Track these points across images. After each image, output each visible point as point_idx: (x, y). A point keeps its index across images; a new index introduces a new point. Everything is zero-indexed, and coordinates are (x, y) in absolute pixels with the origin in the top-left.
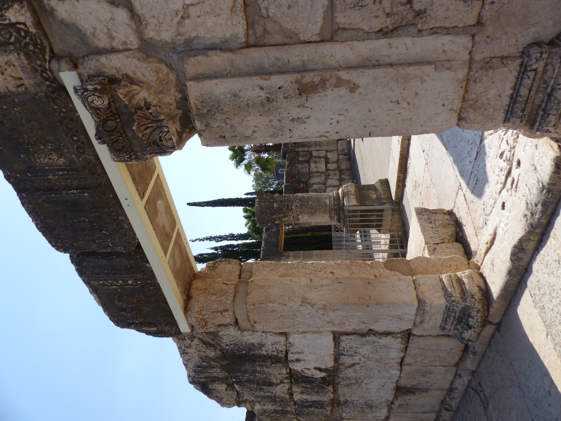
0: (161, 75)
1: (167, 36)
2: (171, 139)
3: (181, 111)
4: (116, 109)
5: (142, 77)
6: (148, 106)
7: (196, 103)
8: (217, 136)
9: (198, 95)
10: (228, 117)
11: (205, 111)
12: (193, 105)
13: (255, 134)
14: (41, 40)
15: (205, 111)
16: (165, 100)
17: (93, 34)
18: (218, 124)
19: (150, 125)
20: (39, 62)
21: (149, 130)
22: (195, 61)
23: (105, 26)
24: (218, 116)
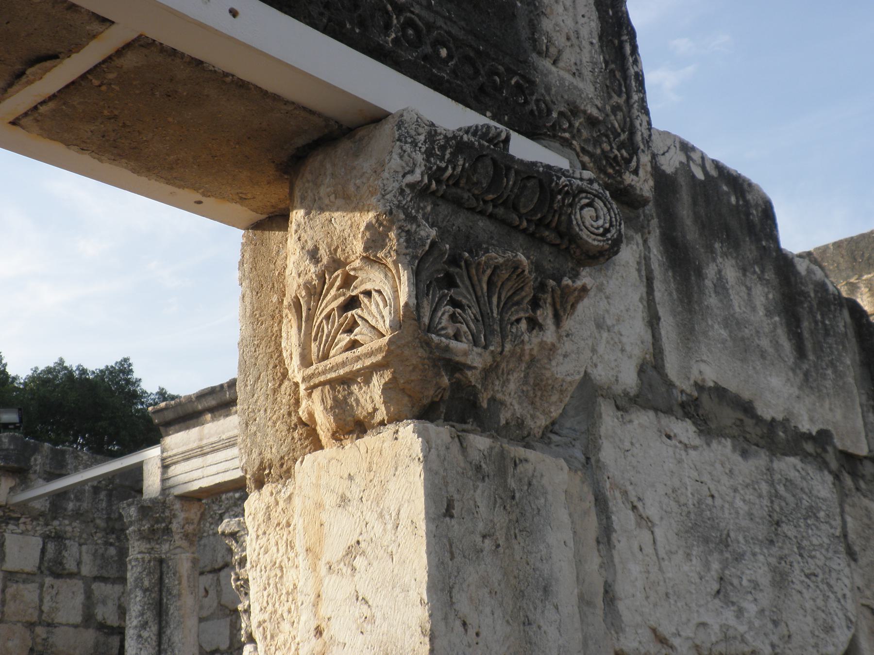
1: (607, 454)
2: (457, 337)
8: (452, 489)
10: (501, 550)
13: (458, 624)
18: (483, 509)
19: (495, 300)
24: (501, 519)
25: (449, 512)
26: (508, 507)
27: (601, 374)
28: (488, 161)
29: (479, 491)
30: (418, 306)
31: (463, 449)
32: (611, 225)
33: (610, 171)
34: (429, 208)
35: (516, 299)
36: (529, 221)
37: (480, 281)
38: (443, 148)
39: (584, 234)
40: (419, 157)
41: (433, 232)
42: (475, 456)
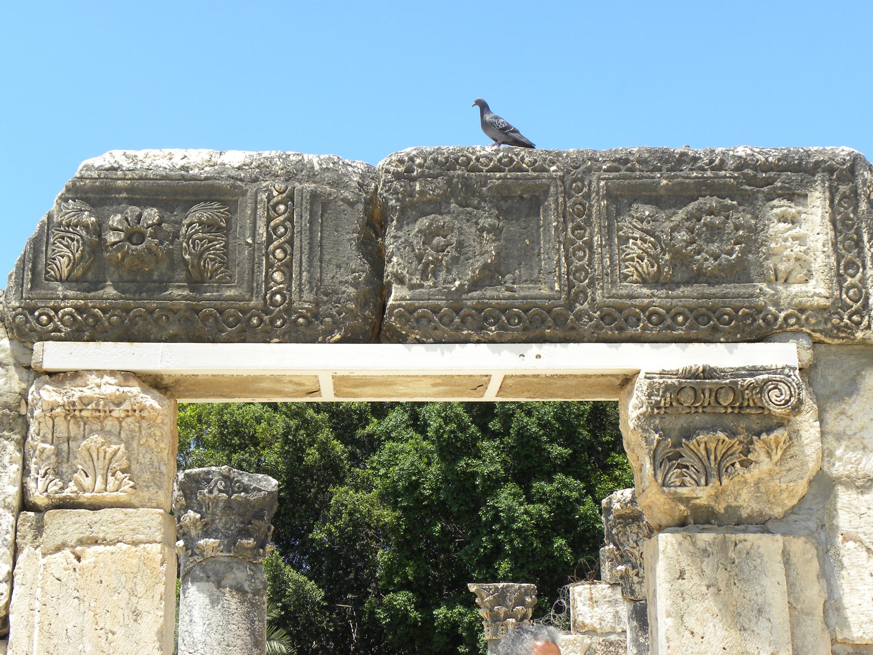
0: (785, 495)
2: (683, 484)
3: (722, 511)
4: (750, 414)
5: (788, 467)
6: (746, 464)
7: (745, 543)
8: (683, 564)
9: (761, 550)
10: (722, 592)
11: (732, 554)
12: (741, 536)
13: (687, 634)
14: (843, 338)
15: (732, 554)
16: (745, 490)
17: (843, 413)
19: (712, 457)
20: (813, 321)
21: (704, 453)
22: (810, 556)
23: (855, 434)
25: (681, 576)
26: (729, 569)
27: (838, 469)
28: (688, 390)
29: (705, 563)
30: (655, 475)
31: (694, 544)
32: (791, 396)
33: (844, 335)
34: (657, 422)
35: (729, 453)
36: (733, 408)
37: (698, 450)
38: (658, 390)
39: (772, 407)
40: (644, 398)
41: (657, 436)
42: (701, 544)
